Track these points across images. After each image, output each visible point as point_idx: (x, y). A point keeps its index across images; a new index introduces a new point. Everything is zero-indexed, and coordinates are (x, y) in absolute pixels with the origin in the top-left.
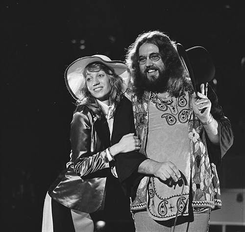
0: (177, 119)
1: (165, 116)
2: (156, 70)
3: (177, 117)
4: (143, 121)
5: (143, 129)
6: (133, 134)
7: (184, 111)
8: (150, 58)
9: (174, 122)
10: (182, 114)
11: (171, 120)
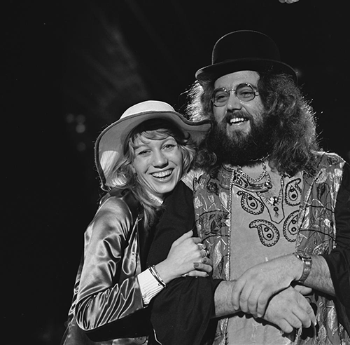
0: (281, 233)
1: (257, 224)
2: (246, 119)
4: (216, 228)
5: (215, 245)
6: (191, 233)
7: (295, 214)
8: (236, 93)
9: (275, 239)
10: (292, 221)
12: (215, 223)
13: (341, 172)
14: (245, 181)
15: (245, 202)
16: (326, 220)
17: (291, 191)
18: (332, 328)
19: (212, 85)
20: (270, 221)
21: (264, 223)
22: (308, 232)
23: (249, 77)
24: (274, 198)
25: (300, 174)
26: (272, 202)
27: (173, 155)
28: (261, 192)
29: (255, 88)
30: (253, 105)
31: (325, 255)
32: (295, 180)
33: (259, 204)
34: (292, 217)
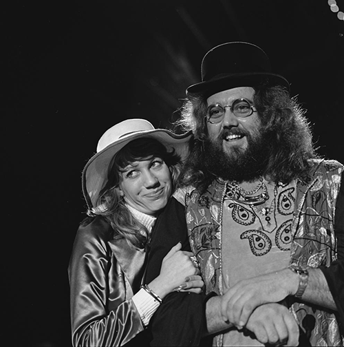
0: (273, 242)
1: (249, 234)
3: (272, 237)
4: (207, 242)
5: (207, 259)
7: (289, 223)
8: (232, 109)
9: (267, 248)
10: (285, 230)
11: (260, 245)
12: (205, 237)
13: (340, 177)
15: (236, 214)
16: (322, 228)
17: (284, 200)
18: (333, 341)
19: (205, 101)
21: (256, 233)
22: (302, 240)
23: (244, 93)
24: (266, 209)
25: (294, 184)
26: (264, 213)
27: (161, 172)
28: (255, 205)
29: (251, 102)
30: (249, 121)
31: (322, 266)
32: (289, 189)
33: (251, 215)
34: (285, 226)
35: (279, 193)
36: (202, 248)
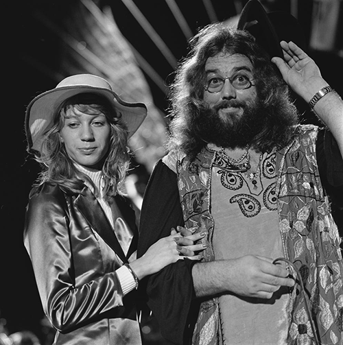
0: (262, 203)
1: (238, 198)
3: (260, 199)
4: (199, 207)
7: (274, 186)
9: (256, 210)
11: (250, 207)
14: (226, 162)
15: (225, 179)
17: (268, 166)
20: (250, 194)
21: (244, 197)
24: (254, 174)
28: (242, 172)
35: (264, 159)
36: (194, 213)
